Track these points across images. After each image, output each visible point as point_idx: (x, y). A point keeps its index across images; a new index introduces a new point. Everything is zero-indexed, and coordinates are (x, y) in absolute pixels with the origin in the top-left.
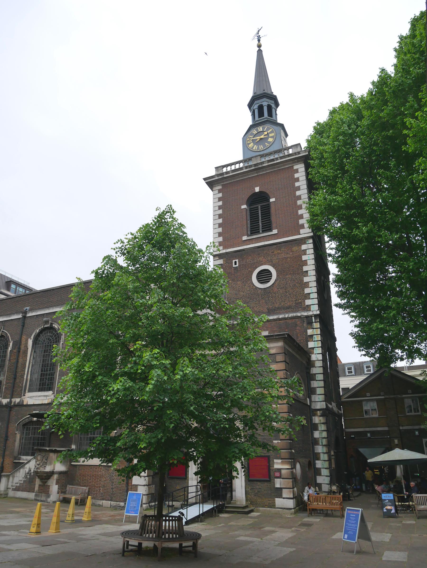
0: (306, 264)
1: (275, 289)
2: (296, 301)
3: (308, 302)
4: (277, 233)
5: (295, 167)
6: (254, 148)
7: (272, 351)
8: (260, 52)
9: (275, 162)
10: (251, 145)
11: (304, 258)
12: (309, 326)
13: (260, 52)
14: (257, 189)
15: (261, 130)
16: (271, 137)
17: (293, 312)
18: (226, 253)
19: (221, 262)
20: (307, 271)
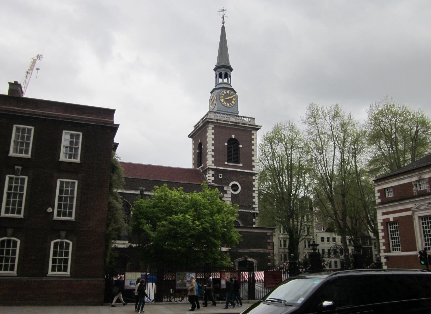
0: (254, 187)
1: (240, 196)
2: (249, 204)
3: (254, 206)
4: (242, 165)
5: (253, 132)
6: (224, 103)
7: (268, 234)
8: (223, 28)
9: (245, 126)
10: (222, 100)
11: (254, 183)
12: (254, 218)
13: (223, 28)
14: (233, 137)
15: (229, 93)
16: (234, 101)
17: (248, 209)
18: (216, 169)
19: (213, 173)
20: (254, 191)
